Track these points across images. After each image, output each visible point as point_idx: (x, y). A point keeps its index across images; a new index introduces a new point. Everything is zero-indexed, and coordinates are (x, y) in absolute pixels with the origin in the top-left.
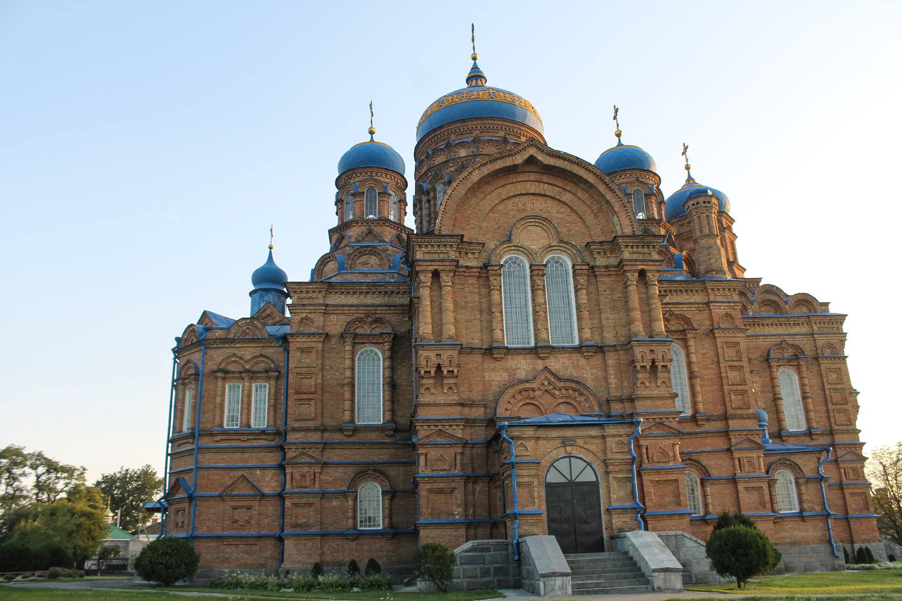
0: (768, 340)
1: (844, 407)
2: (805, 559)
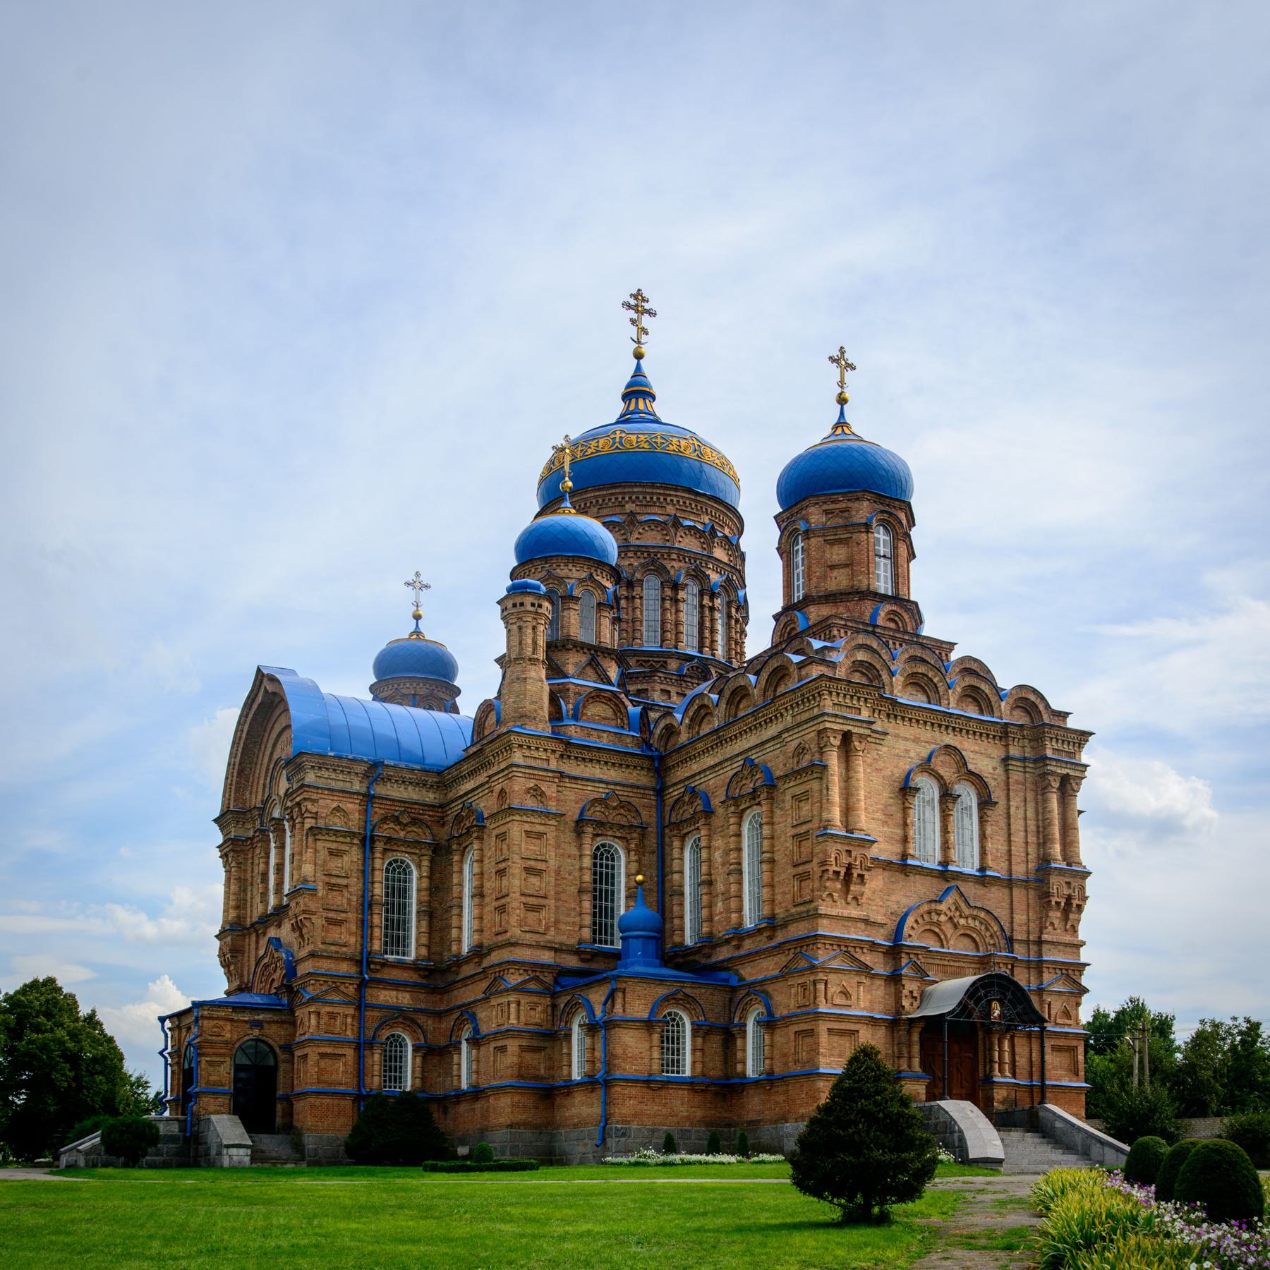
0: (736, 765)
1: (807, 867)
2: (581, 1149)
